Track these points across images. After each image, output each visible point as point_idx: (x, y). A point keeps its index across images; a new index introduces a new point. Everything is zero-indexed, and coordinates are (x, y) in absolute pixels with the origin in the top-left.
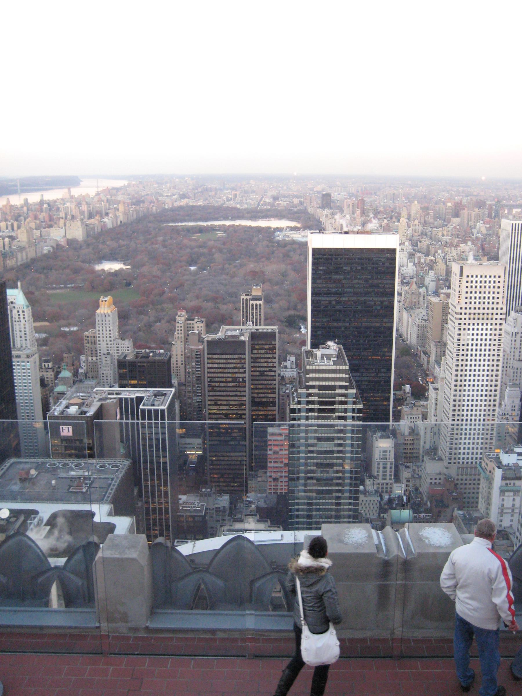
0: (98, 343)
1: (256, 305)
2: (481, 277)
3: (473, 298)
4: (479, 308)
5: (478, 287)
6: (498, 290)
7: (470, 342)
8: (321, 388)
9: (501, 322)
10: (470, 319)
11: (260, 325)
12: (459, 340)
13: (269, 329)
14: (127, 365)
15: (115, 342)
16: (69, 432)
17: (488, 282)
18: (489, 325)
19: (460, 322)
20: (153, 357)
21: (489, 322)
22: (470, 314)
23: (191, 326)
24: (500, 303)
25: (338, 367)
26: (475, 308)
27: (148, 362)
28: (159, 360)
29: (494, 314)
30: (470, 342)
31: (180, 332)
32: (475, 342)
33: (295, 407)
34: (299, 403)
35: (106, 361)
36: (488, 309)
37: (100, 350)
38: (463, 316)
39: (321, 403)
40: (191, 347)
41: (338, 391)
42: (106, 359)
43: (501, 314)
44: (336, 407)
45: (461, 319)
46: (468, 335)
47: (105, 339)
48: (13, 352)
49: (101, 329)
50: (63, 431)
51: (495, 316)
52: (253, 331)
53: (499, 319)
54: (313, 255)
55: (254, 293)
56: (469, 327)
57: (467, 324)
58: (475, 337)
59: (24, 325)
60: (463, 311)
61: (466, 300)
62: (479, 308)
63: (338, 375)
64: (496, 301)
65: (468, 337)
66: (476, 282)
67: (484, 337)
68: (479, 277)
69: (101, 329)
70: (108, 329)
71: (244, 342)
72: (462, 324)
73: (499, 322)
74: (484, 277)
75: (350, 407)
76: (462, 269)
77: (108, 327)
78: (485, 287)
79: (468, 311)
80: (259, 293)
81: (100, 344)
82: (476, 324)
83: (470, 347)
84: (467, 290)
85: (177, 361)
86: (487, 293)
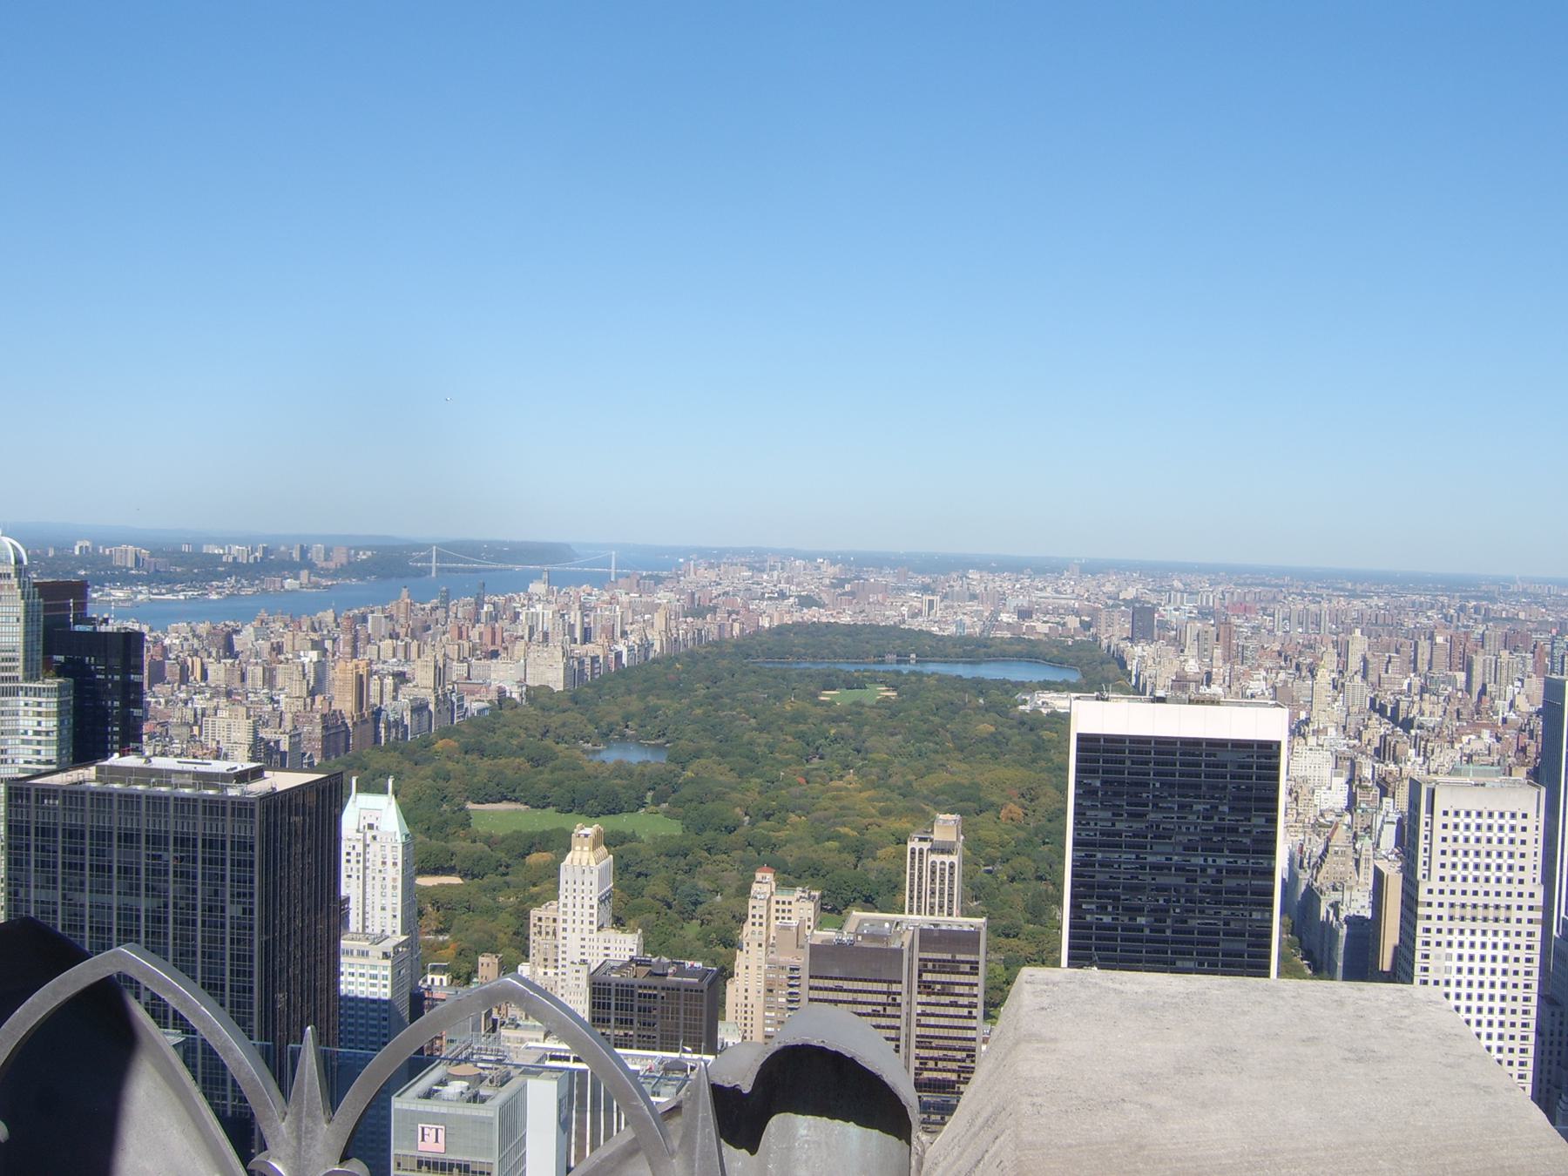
0: (561, 934)
1: (943, 863)
2: (1479, 814)
3: (1460, 867)
4: (1475, 893)
5: (1472, 840)
6: (1523, 849)
7: (1454, 977)
9: (1531, 928)
10: (1451, 918)
11: (950, 914)
12: (1426, 969)
14: (613, 992)
15: (602, 935)
16: (437, 1141)
17: (1495, 828)
18: (1501, 934)
19: (1427, 924)
20: (675, 975)
21: (1501, 926)
22: (1452, 905)
23: (787, 907)
24: (1528, 881)
26: (1464, 893)
27: (663, 989)
28: (690, 983)
29: (1514, 908)
30: (1454, 977)
31: (757, 920)
32: (1465, 977)
35: (577, 979)
36: (1498, 894)
37: (564, 952)
38: (1434, 911)
40: (782, 959)
42: (577, 975)
43: (1531, 908)
45: (1429, 917)
46: (1449, 957)
47: (578, 925)
48: (342, 942)
49: (570, 901)
50: (423, 1140)
51: (1515, 914)
52: (926, 927)
53: (1525, 921)
54: (1079, 749)
55: (938, 836)
56: (1450, 938)
57: (1445, 931)
58: (1465, 964)
59: (395, 880)
61: (1443, 872)
62: (1475, 893)
64: (1516, 875)
65: (1448, 964)
66: (1467, 827)
67: (1488, 965)
68: (1474, 814)
69: (570, 901)
70: (587, 903)
71: (899, 952)
72: (1434, 931)
73: (1525, 927)
74: (1485, 814)
77: (587, 899)
78: (1489, 841)
80: (950, 836)
81: (564, 938)
82: (1467, 932)
84: (1444, 846)
85: (746, 990)
86: (1494, 854)
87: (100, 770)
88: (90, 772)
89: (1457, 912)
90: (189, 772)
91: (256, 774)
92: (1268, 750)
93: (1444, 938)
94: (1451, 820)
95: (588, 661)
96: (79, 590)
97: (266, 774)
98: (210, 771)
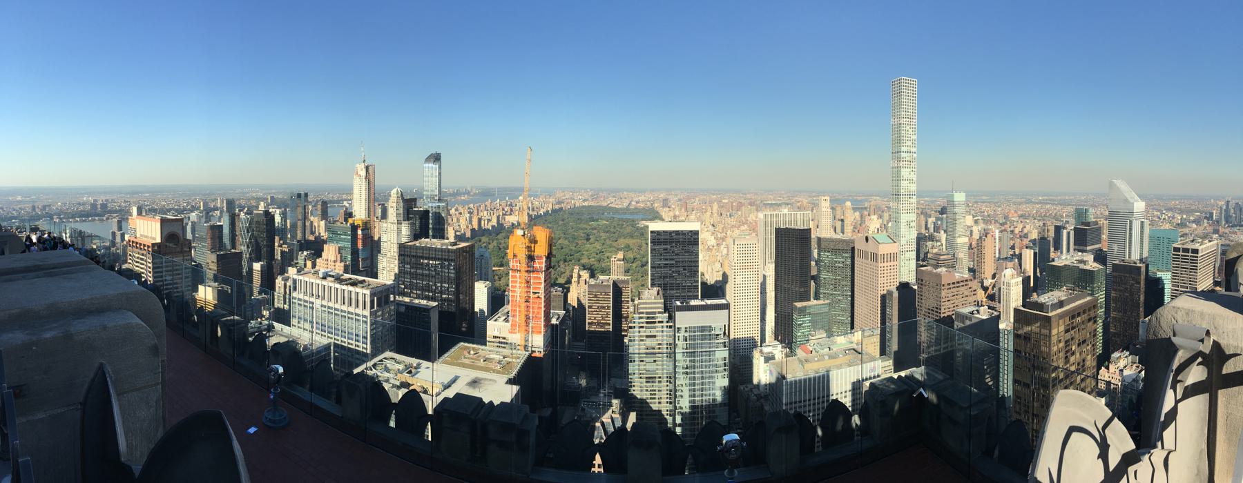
7: (742, 283)
8: (647, 313)
13: (626, 278)
21: (751, 270)
25: (657, 301)
30: (742, 283)
33: (630, 325)
34: (634, 322)
39: (647, 323)
41: (657, 315)
44: (656, 325)
51: (754, 267)
58: (744, 279)
60: (736, 265)
63: (657, 306)
73: (757, 270)
75: (665, 324)
76: (734, 240)
79: (739, 265)
83: (741, 285)
89: (742, 267)
92: (696, 233)
93: (739, 274)
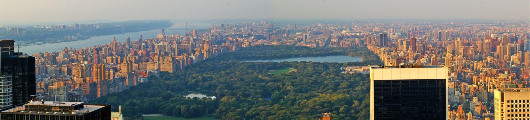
2: (520, 101)
66: (516, 106)
68: (518, 101)
84: (509, 113)
87: (26, 107)
88: (23, 108)
90: (58, 106)
91: (80, 107)
94: (510, 104)
95: (181, 61)
96: (11, 43)
97: (84, 106)
98: (65, 106)
